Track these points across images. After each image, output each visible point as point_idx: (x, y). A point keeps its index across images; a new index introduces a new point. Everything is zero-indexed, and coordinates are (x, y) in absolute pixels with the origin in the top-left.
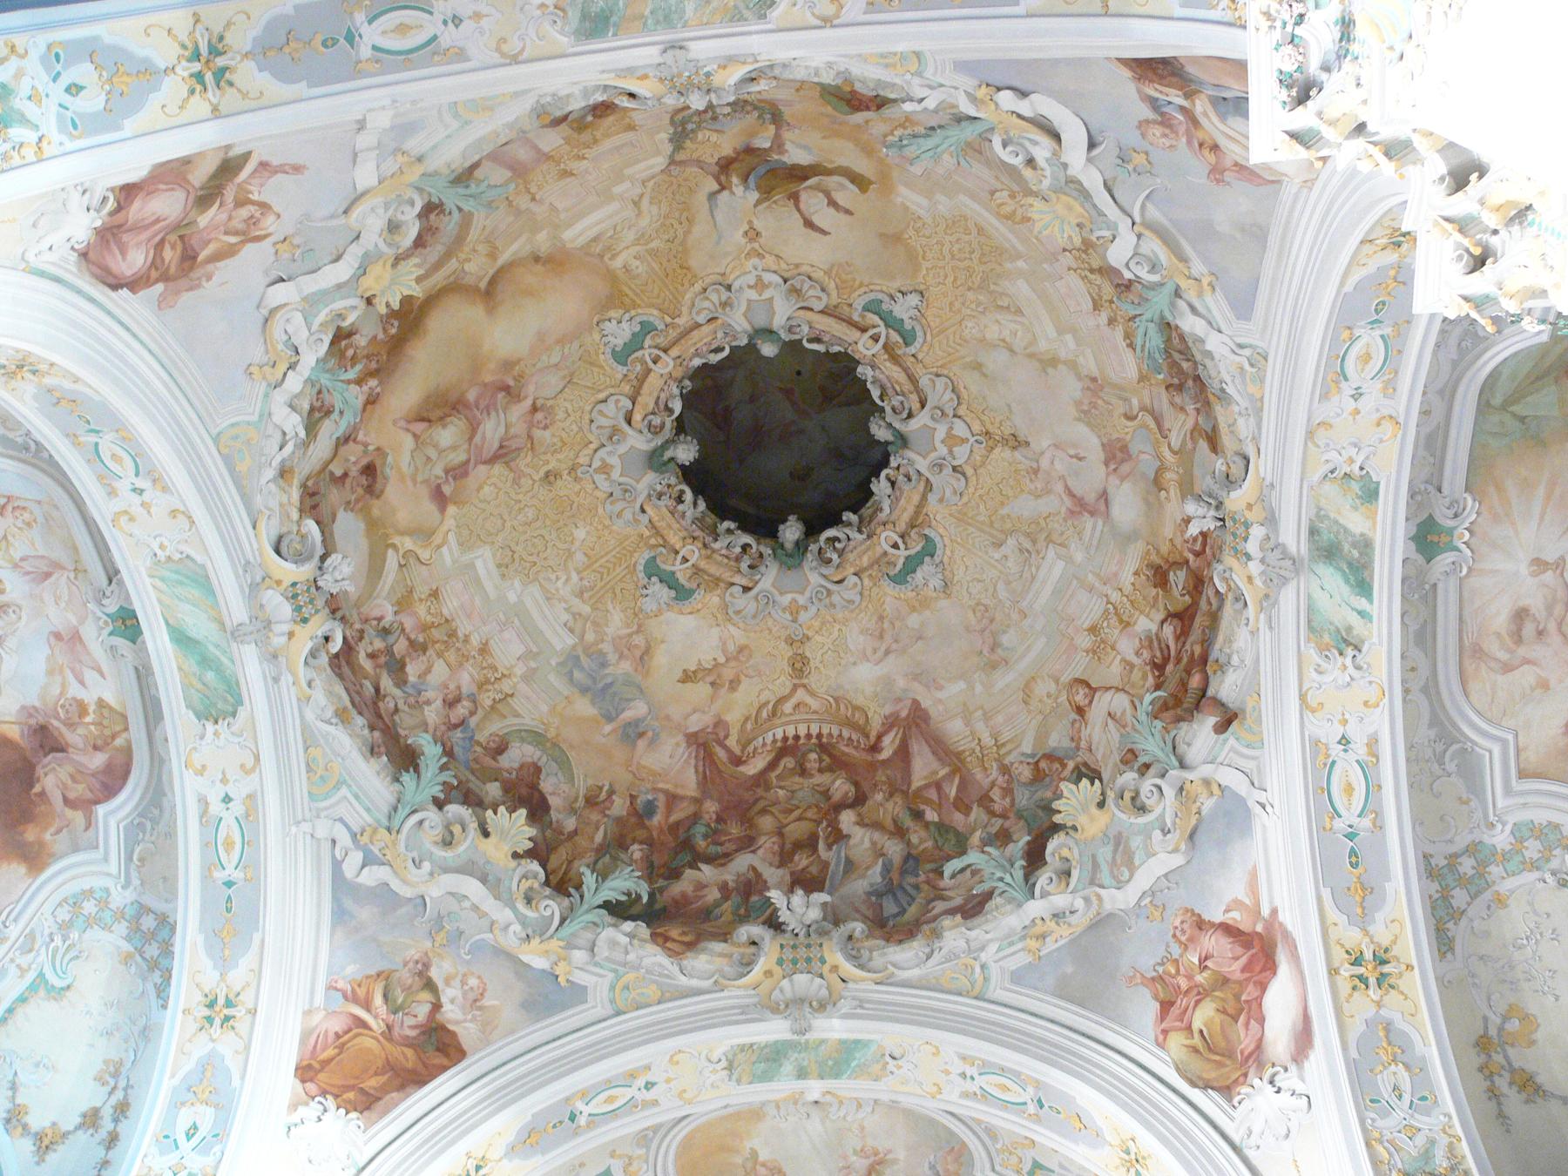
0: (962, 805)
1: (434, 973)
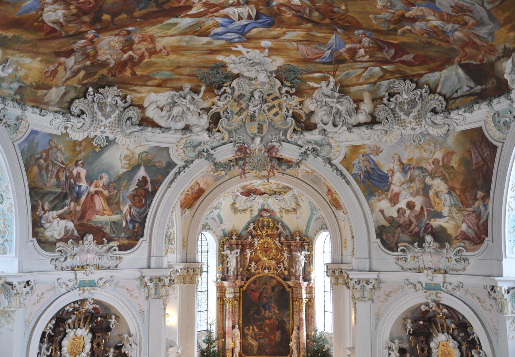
1: (198, 182)
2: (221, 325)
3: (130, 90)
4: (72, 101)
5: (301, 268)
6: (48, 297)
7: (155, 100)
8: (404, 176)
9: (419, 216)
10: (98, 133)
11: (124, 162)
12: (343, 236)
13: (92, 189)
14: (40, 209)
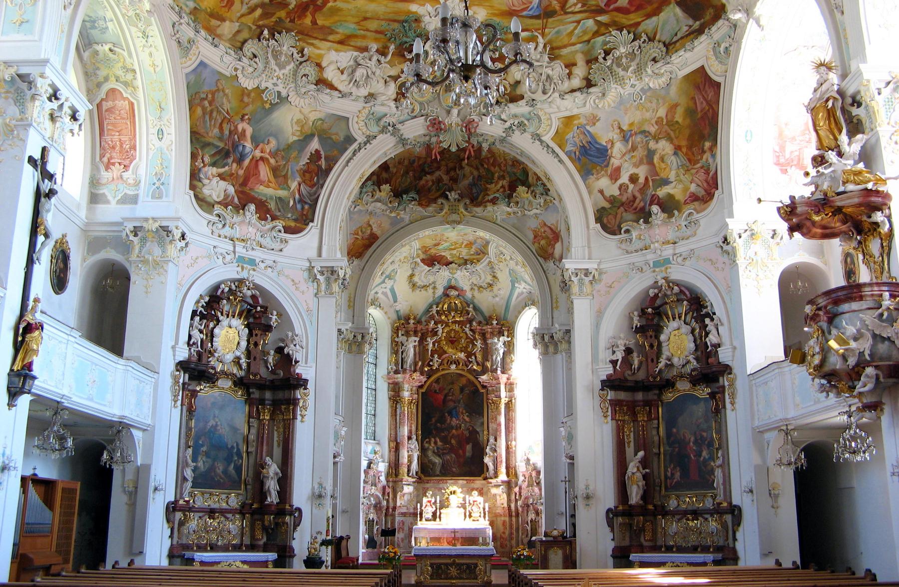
0: (494, 165)
2: (393, 433)
3: (308, 43)
4: (245, 41)
5: (499, 359)
6: (203, 264)
7: (335, 60)
8: (624, 145)
9: (643, 190)
10: (270, 86)
11: (296, 128)
12: (554, 294)
13: (258, 153)
14: (200, 160)
